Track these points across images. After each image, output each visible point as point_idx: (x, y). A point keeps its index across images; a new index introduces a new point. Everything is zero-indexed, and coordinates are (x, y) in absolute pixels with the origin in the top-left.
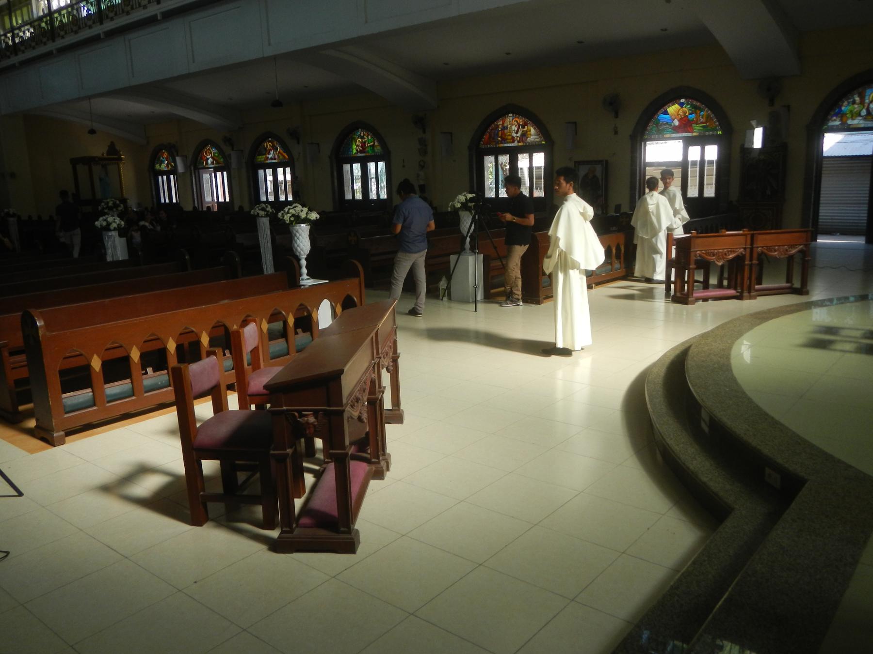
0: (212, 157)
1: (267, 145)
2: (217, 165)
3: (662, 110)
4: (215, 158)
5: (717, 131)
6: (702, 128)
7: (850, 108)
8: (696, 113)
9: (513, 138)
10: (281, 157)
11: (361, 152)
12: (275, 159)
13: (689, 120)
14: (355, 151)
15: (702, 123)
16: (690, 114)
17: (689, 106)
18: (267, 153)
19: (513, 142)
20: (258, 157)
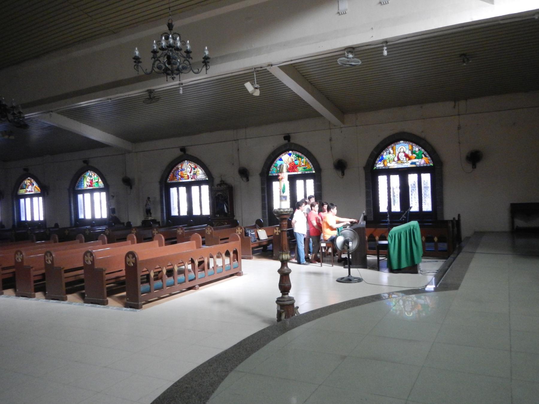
1: (27, 183)
3: (279, 158)
5: (312, 171)
6: (303, 169)
7: (388, 156)
8: (299, 160)
9: (188, 176)
10: (36, 190)
11: (90, 186)
12: (32, 191)
13: (295, 164)
14: (85, 186)
15: (303, 166)
16: (296, 160)
17: (294, 155)
18: (27, 187)
19: (188, 178)
20: (20, 190)
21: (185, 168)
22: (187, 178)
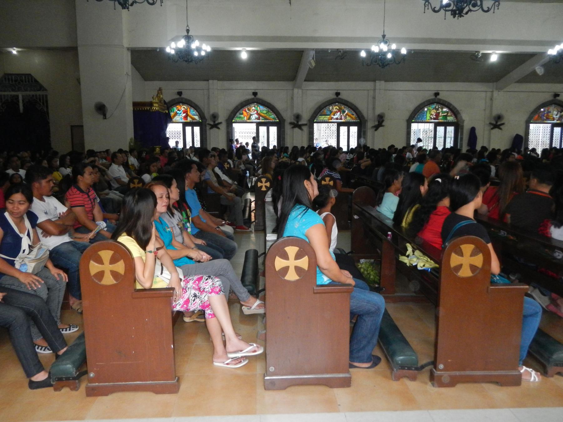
0: (257, 114)
2: (263, 121)
4: (262, 114)
11: (434, 119)
12: (341, 119)
14: (428, 118)
18: (332, 114)
20: (320, 117)
21: (552, 111)
22: (552, 119)
